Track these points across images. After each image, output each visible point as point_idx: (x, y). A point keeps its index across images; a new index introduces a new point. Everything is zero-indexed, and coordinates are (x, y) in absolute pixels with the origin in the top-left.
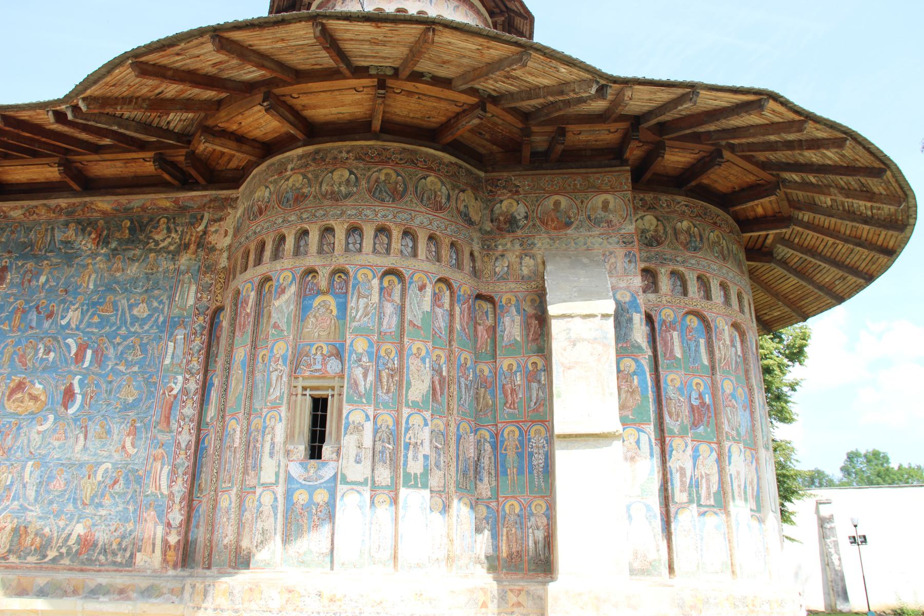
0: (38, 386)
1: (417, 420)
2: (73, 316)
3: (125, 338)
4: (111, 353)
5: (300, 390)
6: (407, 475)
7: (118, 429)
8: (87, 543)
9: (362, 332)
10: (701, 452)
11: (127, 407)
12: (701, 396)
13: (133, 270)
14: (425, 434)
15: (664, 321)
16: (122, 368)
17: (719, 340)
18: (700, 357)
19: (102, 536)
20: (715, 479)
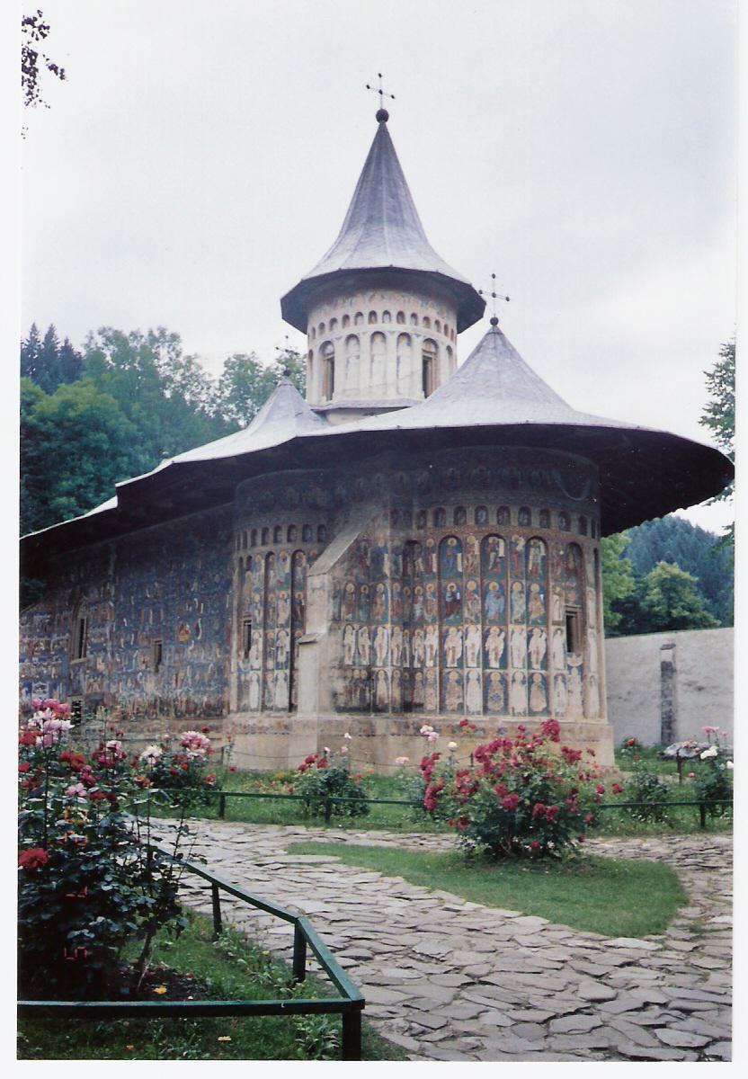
0: (188, 626)
1: (283, 634)
2: (195, 584)
3: (213, 595)
4: (209, 605)
5: (242, 624)
6: (277, 664)
7: (214, 645)
8: (208, 706)
9: (257, 590)
10: (450, 633)
11: (217, 633)
12: (453, 595)
13: (213, 556)
14: (287, 641)
15: (428, 548)
16: (213, 612)
17: (468, 553)
18: (457, 565)
19: (213, 702)
20: (459, 650)
